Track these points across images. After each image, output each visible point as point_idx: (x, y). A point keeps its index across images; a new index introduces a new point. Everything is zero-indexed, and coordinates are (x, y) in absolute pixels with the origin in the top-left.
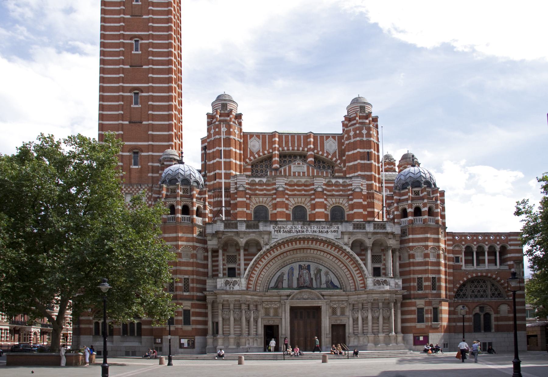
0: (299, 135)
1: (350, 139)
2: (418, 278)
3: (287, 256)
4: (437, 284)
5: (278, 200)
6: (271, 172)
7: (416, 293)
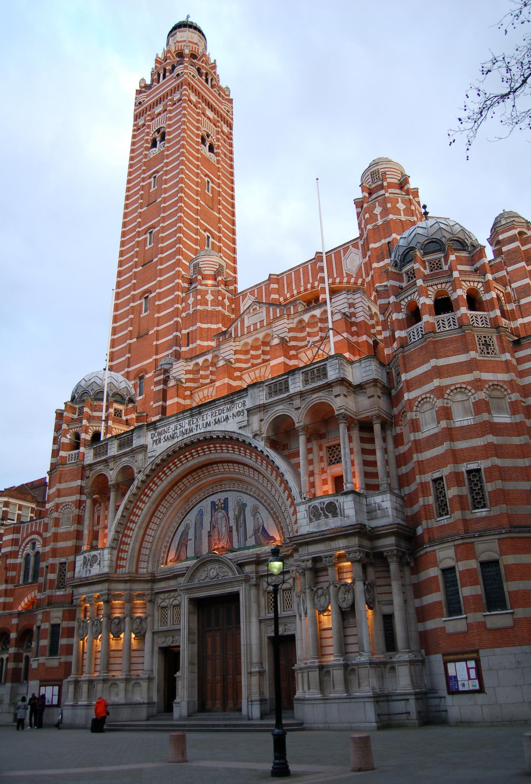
0: (304, 265)
2: (435, 481)
3: (187, 488)
4: (489, 487)
7: (436, 525)
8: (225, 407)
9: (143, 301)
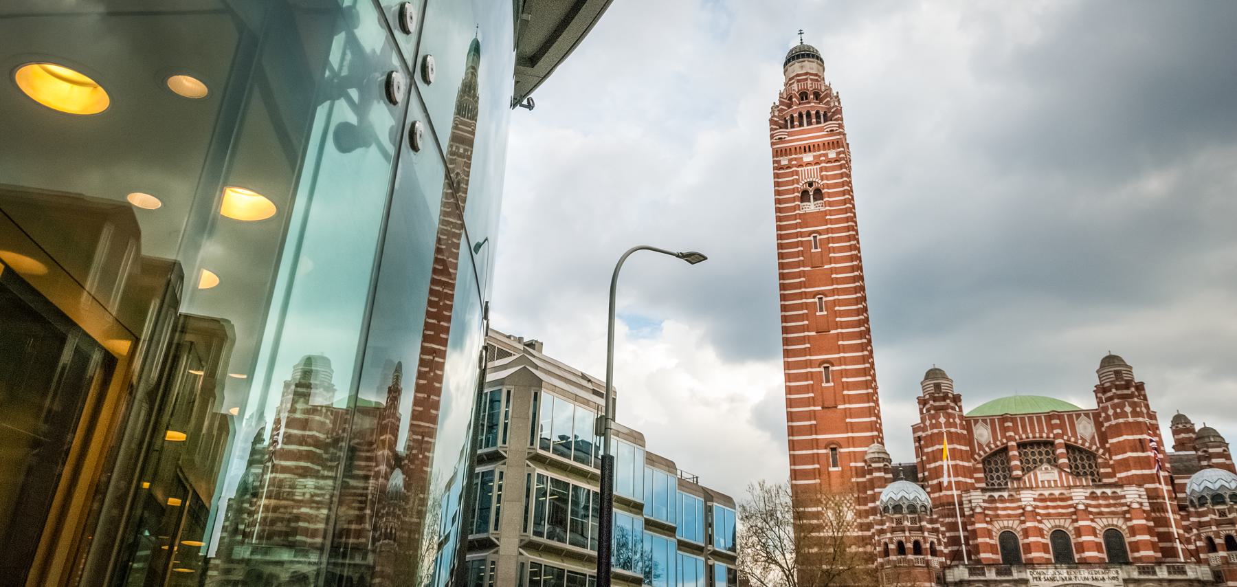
1: (1110, 420)
5: (1029, 524)
6: (1013, 482)
8: (1101, 570)
9: (822, 369)
